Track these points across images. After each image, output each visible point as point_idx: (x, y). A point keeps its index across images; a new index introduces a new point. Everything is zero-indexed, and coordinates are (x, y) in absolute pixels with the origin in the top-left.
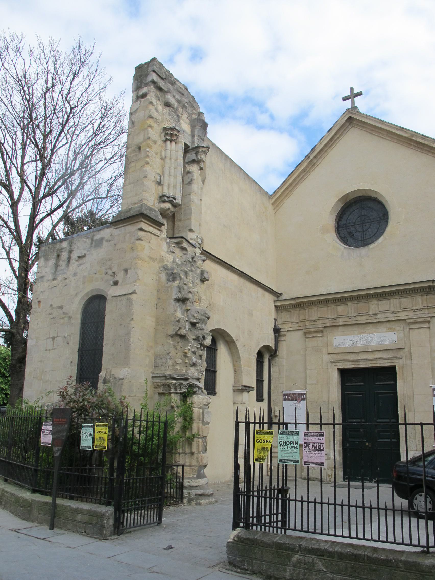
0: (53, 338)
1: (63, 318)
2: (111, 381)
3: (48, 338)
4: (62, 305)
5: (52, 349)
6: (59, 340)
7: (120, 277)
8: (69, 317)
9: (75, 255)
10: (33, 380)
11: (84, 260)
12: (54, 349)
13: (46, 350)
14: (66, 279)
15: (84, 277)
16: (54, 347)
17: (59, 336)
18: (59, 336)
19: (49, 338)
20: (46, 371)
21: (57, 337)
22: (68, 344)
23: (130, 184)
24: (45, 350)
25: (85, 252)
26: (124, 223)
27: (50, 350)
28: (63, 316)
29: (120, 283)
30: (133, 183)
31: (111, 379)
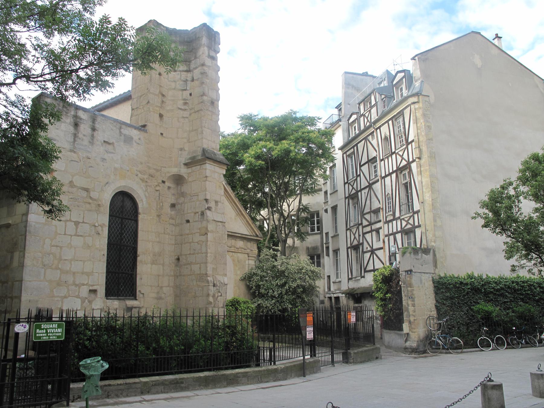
0: (77, 223)
1: (89, 203)
2: (218, 285)
3: (68, 221)
4: (89, 187)
5: (75, 235)
6: (87, 227)
7: (212, 204)
8: (99, 205)
9: (100, 136)
10: (42, 268)
11: (110, 148)
12: (78, 236)
13: (65, 234)
14: (89, 158)
15: (115, 169)
16: (78, 234)
17: (86, 223)
18: (86, 223)
19: (70, 220)
20: (66, 260)
21: (83, 222)
22: (99, 234)
23: (208, 128)
24: (64, 233)
25: (114, 141)
26: (214, 163)
27: (71, 236)
28: (91, 201)
29: (213, 209)
30: (211, 130)
31: (218, 283)
